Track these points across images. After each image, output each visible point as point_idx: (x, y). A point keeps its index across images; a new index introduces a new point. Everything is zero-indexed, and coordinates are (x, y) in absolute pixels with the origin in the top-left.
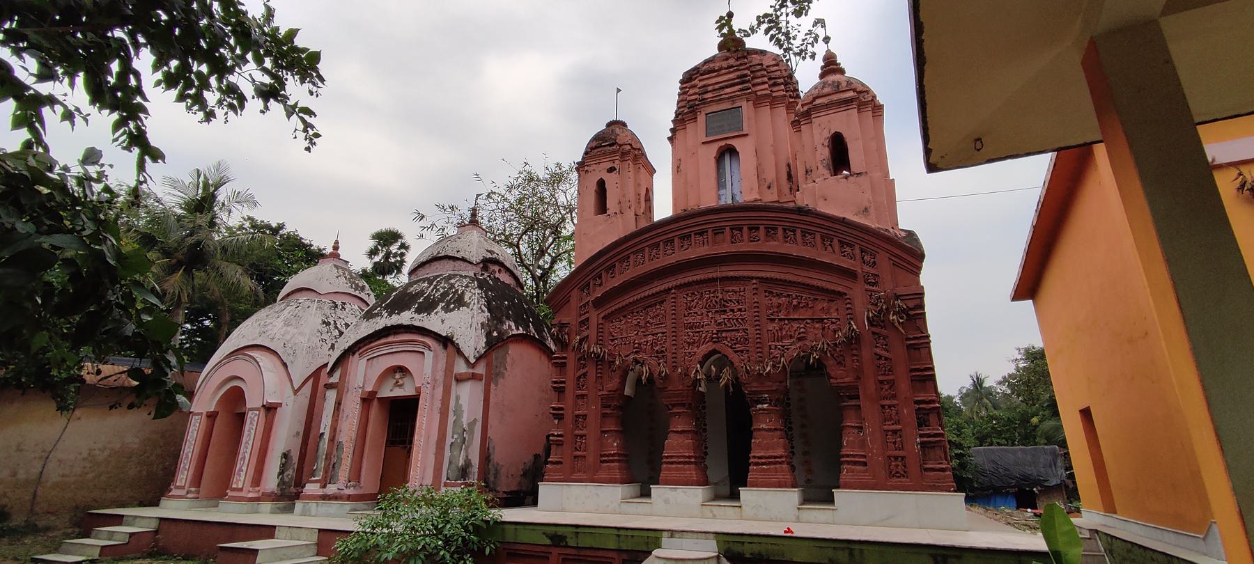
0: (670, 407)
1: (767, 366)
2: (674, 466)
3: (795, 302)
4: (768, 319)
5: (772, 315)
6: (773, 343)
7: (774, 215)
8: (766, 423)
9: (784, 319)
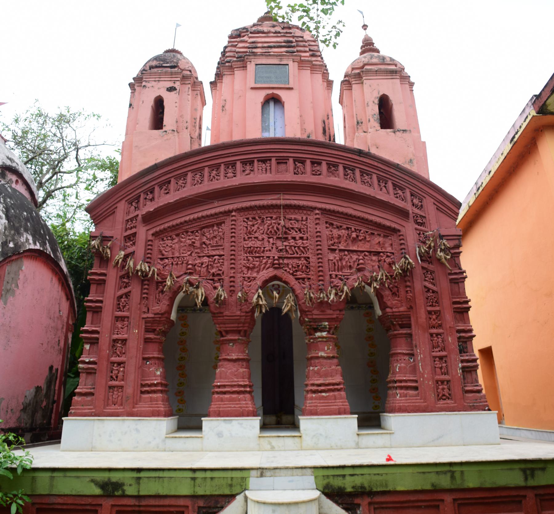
0: (224, 333)
1: (330, 294)
2: (227, 396)
3: (354, 235)
4: (329, 249)
5: (333, 245)
6: (333, 272)
7: (336, 153)
8: (323, 350)
9: (344, 250)
